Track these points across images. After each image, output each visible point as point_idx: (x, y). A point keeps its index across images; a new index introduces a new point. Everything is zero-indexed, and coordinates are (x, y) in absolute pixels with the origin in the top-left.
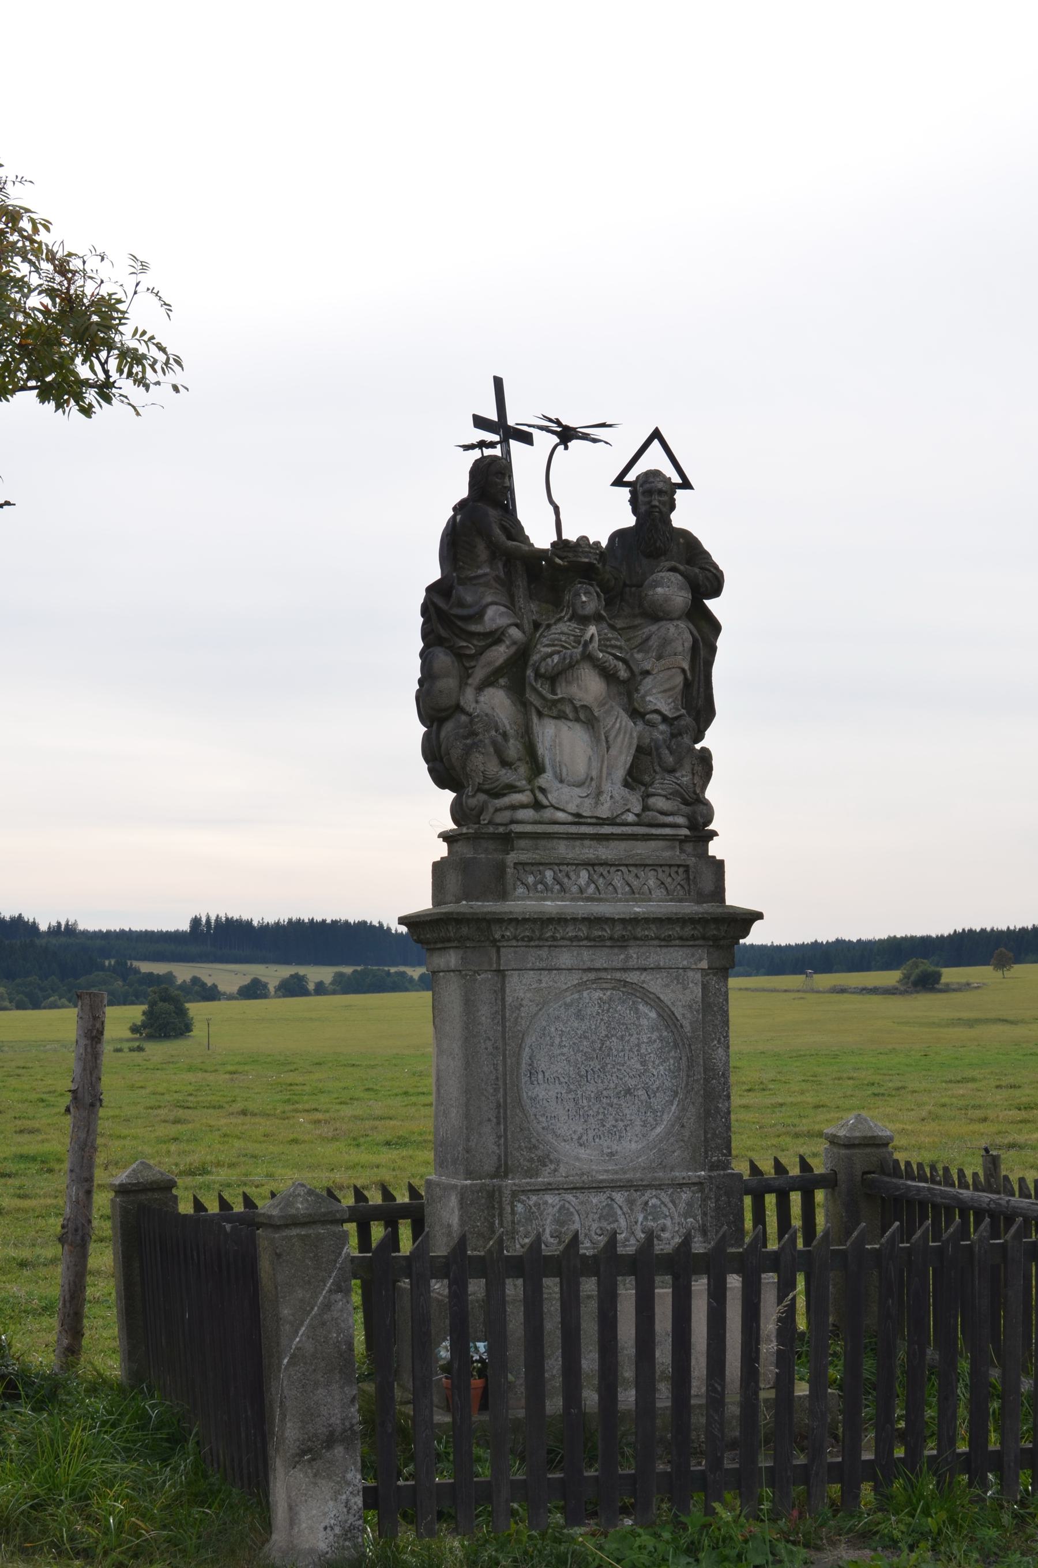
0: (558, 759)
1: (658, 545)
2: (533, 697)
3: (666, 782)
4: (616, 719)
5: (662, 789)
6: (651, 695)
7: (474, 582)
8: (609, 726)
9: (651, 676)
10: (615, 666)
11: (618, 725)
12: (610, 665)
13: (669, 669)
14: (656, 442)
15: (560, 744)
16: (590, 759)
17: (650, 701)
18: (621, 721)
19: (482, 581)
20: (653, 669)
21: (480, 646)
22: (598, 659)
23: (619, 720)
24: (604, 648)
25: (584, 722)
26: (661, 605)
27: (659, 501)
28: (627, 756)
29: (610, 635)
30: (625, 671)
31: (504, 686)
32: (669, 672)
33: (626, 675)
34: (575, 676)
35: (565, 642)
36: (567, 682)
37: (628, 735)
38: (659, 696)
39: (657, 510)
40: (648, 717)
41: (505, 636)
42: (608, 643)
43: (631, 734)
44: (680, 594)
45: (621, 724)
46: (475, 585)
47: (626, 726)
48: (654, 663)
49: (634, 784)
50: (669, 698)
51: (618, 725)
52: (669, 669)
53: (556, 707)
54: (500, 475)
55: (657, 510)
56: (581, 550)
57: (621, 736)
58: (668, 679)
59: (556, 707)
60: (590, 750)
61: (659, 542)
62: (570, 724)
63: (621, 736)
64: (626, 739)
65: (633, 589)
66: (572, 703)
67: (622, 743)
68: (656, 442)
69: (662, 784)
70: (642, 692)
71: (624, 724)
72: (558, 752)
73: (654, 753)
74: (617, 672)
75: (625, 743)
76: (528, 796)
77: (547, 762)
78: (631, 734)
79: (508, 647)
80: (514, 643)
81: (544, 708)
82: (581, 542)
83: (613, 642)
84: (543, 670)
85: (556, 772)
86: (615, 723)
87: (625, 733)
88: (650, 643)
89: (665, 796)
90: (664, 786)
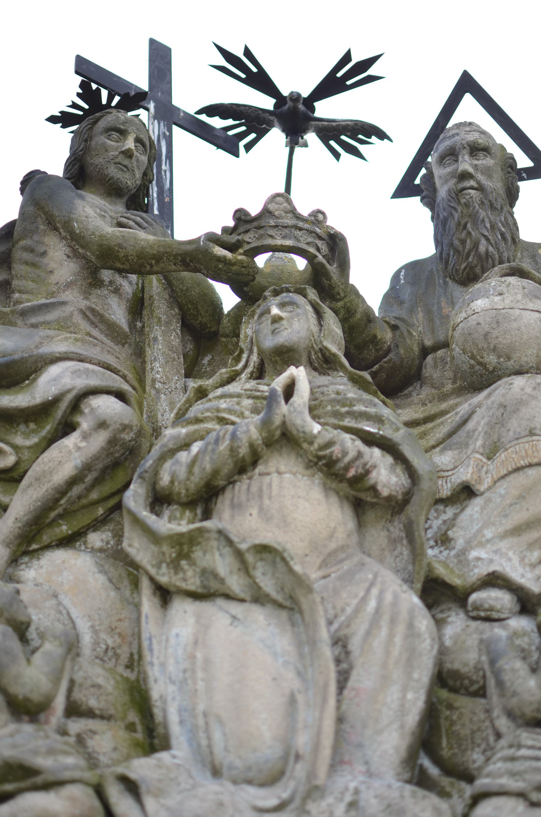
0: (201, 707)
1: (482, 248)
2: (136, 544)
3: (523, 752)
4: (368, 591)
5: (513, 774)
6: (481, 545)
7: (33, 320)
8: (349, 610)
9: (477, 502)
10: (360, 455)
11: (372, 604)
12: (345, 453)
13: (518, 469)
14: (468, 99)
15: (207, 661)
16: (292, 701)
17: (478, 559)
18: (382, 592)
19: (51, 316)
20: (480, 480)
21: (30, 448)
22: (311, 439)
23: (375, 591)
24: (333, 421)
25: (281, 606)
26: (486, 335)
27: (476, 167)
28: (404, 690)
29: (350, 395)
30: (392, 469)
31: (101, 550)
32: (519, 479)
33: (394, 479)
34: (254, 489)
35: (230, 411)
36: (233, 506)
37: (401, 629)
38: (504, 545)
39: (472, 183)
40: (474, 597)
41: (82, 413)
42: (344, 410)
43: (411, 626)
44: (531, 306)
45: (380, 599)
46: (34, 326)
47: (395, 603)
48: (479, 468)
49: (445, 781)
50: (531, 546)
51: (372, 604)
52: (518, 469)
53: (193, 563)
54: (115, 135)
55: (472, 183)
56: (272, 223)
57: (384, 632)
58: (522, 497)
59: (193, 563)
60: (291, 675)
61: (483, 241)
62: (235, 608)
63: (384, 632)
64: (398, 640)
65: (440, 353)
66: (230, 542)
67: (387, 652)
68: (468, 99)
69: (513, 759)
70: (460, 543)
71: (388, 597)
72: (200, 685)
73: (491, 683)
74: (368, 472)
75: (396, 651)
76: (72, 799)
77: (173, 718)
78: (411, 626)
79: (85, 437)
80: (102, 425)
81: (158, 566)
82: (271, 207)
83: (359, 408)
84: (165, 479)
85: (199, 746)
86: (364, 600)
87: (393, 621)
88: (470, 425)
89: (521, 795)
90: (518, 766)
